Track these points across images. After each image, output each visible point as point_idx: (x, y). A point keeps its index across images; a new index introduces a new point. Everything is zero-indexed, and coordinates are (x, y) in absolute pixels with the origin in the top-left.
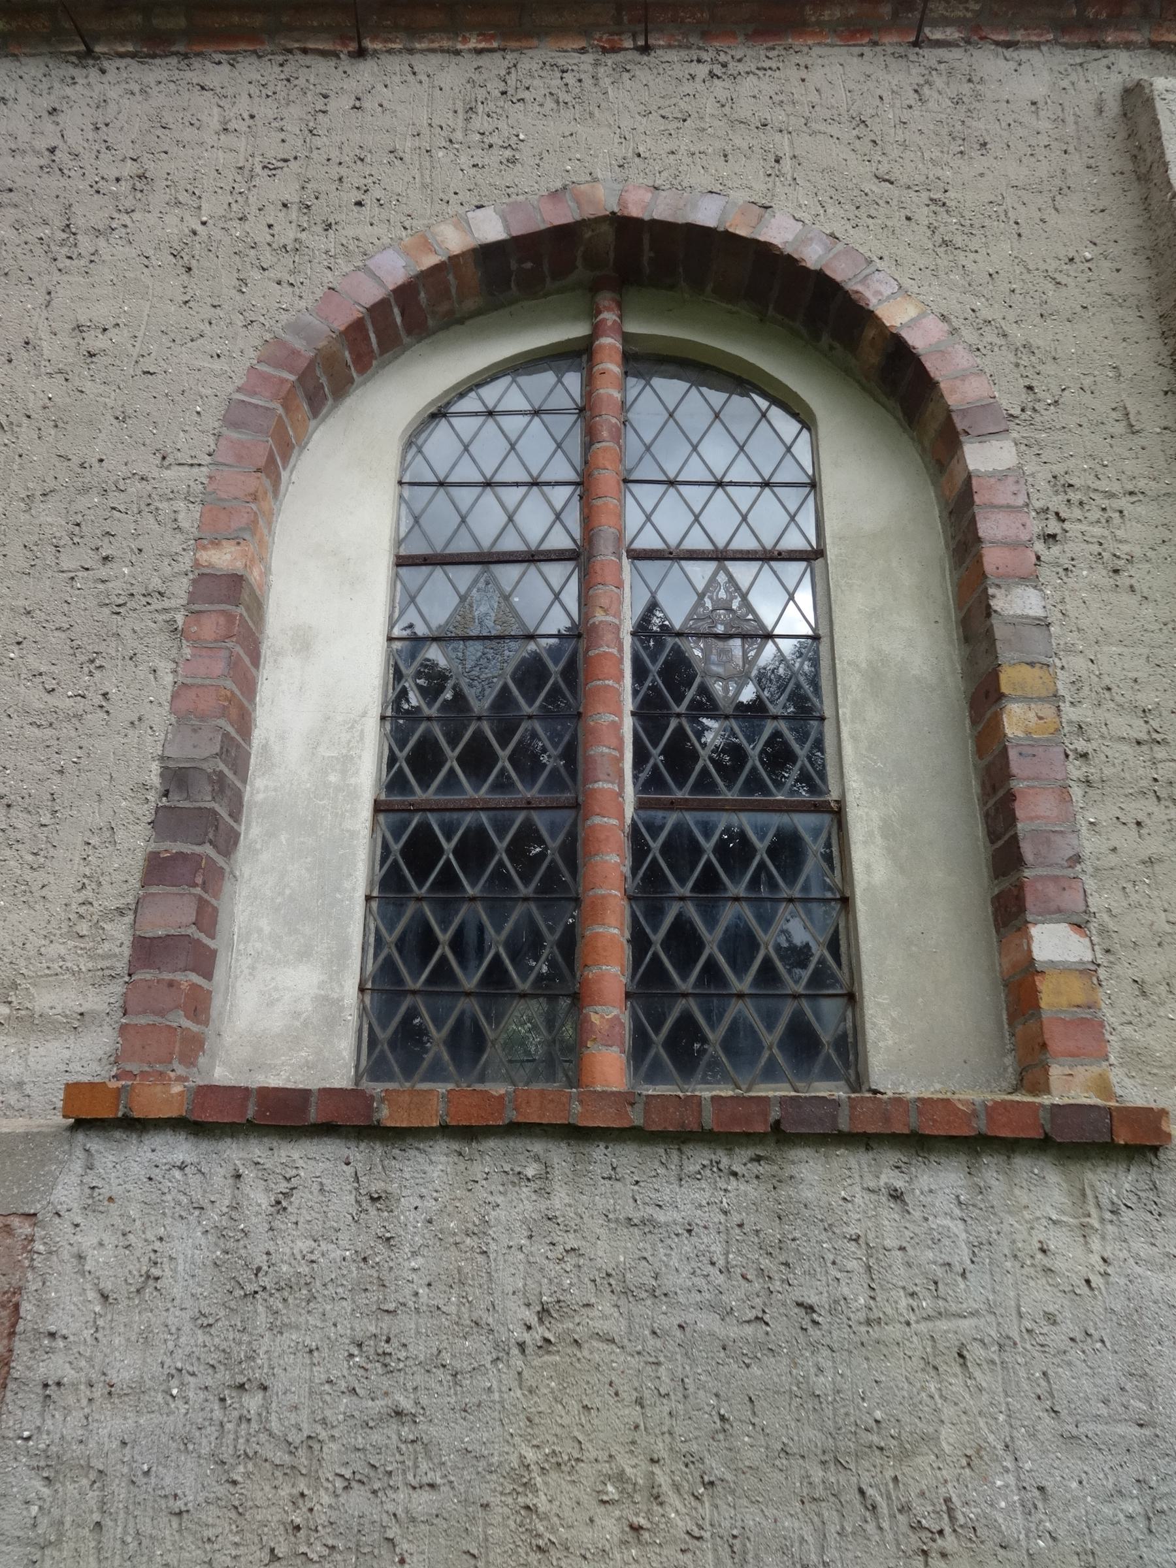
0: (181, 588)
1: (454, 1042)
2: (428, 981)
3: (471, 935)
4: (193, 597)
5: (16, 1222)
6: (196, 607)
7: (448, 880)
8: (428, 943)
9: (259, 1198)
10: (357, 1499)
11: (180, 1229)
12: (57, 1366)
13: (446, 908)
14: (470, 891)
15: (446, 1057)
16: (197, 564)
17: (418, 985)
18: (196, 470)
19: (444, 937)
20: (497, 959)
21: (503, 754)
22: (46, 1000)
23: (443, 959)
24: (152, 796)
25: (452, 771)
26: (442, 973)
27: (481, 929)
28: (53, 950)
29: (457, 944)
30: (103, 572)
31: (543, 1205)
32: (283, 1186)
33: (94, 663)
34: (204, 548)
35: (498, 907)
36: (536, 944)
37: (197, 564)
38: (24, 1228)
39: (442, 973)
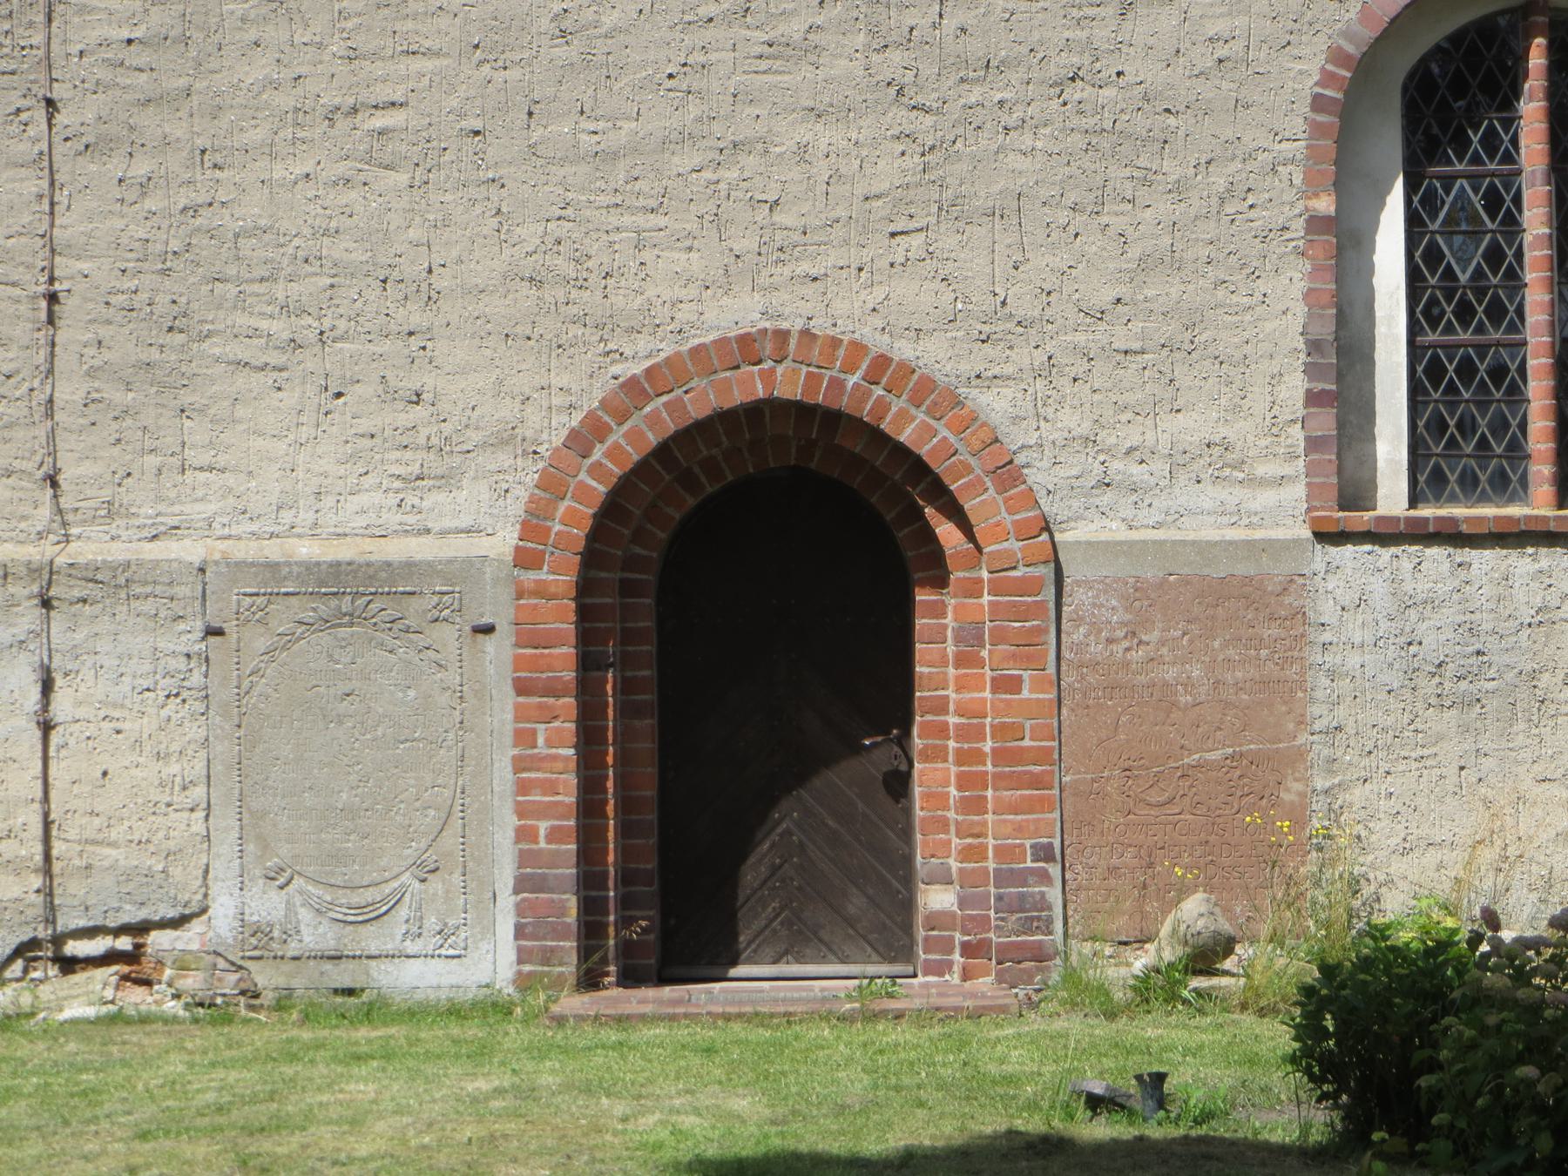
0: (1299, 226)
1: (1462, 481)
2: (1445, 448)
3: (1468, 420)
4: (1308, 231)
5: (1296, 578)
6: (1309, 237)
7: (1451, 389)
8: (1444, 427)
9: (1407, 565)
10: (1463, 685)
11: (1372, 579)
12: (1327, 636)
13: (1452, 406)
14: (1466, 396)
15: (1457, 490)
16: (1307, 209)
17: (1439, 451)
18: (1296, 143)
19: (1452, 423)
20: (1483, 435)
21: (1480, 309)
22: (1261, 470)
23: (1452, 435)
24: (1302, 356)
25: (1449, 321)
26: (1452, 442)
27: (1473, 417)
28: (1263, 443)
29: (1459, 426)
30: (1253, 214)
31: (1537, 566)
32: (1418, 560)
33: (1254, 275)
34: (1310, 198)
35: (1483, 406)
36: (1506, 425)
37: (1307, 209)
38: (1301, 581)
39: (1452, 442)
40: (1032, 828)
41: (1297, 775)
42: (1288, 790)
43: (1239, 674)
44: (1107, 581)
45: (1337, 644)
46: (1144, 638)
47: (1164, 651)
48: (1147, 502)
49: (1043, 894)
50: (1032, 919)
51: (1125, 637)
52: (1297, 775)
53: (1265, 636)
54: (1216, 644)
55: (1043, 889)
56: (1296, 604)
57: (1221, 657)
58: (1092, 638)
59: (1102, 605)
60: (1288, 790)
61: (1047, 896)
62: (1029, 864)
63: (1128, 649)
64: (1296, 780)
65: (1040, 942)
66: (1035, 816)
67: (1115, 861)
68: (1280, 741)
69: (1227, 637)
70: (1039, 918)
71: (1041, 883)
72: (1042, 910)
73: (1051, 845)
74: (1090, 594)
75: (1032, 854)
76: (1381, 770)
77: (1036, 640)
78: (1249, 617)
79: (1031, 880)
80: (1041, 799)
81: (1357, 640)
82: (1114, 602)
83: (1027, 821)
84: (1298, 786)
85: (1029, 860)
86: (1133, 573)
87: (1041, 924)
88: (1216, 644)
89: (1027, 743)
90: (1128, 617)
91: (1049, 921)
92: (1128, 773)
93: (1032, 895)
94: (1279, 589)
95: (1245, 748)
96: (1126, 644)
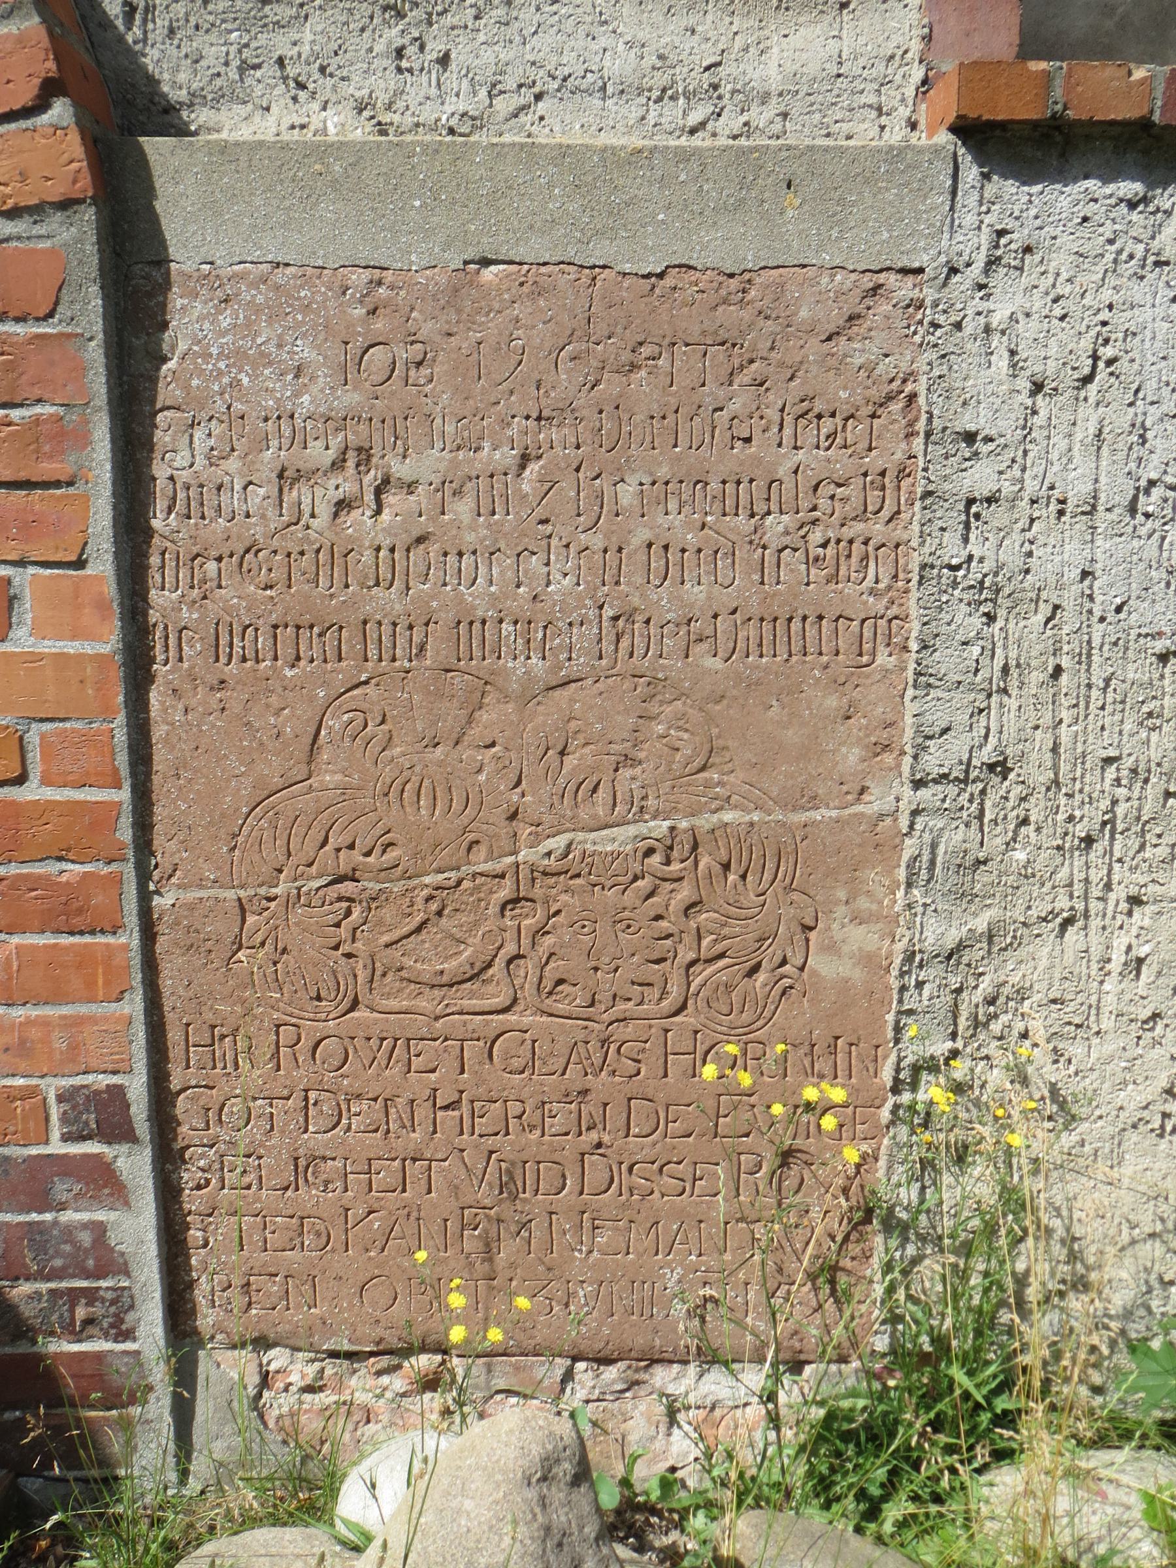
5: (891, 279)
11: (1138, 292)
38: (905, 289)
40: (60, 1044)
41: (863, 903)
42: (832, 948)
43: (696, 593)
44: (280, 276)
45: (1014, 499)
46: (401, 470)
47: (463, 508)
48: (435, 48)
49: (99, 1229)
50: (74, 1295)
51: (338, 465)
52: (863, 903)
53: (783, 471)
54: (627, 493)
55: (100, 1216)
56: (885, 368)
57: (643, 535)
58: (233, 464)
59: (265, 359)
60: (832, 948)
61: (112, 1238)
62: (57, 1147)
63: (342, 506)
64: (858, 919)
65: (99, 1357)
66: (66, 1010)
67: (315, 1140)
68: (814, 802)
69: (663, 472)
70: (91, 1295)
71: (96, 1200)
72: (100, 1273)
73: (117, 1092)
74: (225, 321)
75: (64, 1119)
76: (1119, 893)
77: (48, 469)
78: (735, 406)
79: (62, 1189)
80: (84, 959)
81: (1077, 490)
82: (305, 351)
83: (44, 1023)
84: (861, 937)
85: (55, 1134)
86: (365, 254)
87: (98, 1310)
88: (627, 493)
89: (32, 792)
90: (349, 398)
91: (123, 1303)
92: (347, 888)
93: (68, 1232)
94: (836, 318)
95: (705, 822)
96: (344, 484)
